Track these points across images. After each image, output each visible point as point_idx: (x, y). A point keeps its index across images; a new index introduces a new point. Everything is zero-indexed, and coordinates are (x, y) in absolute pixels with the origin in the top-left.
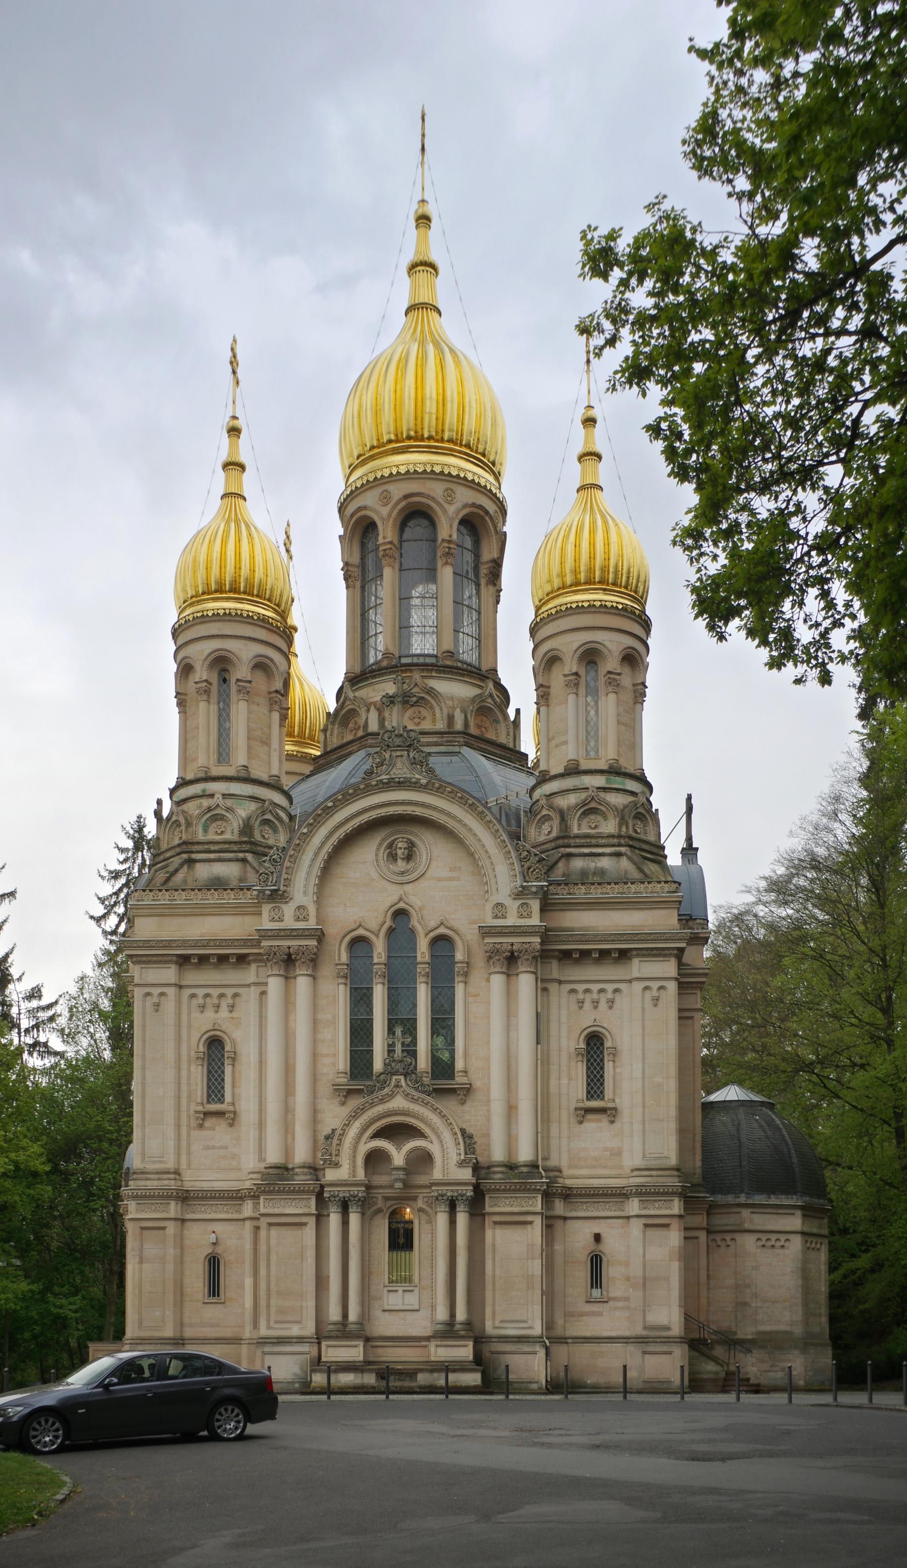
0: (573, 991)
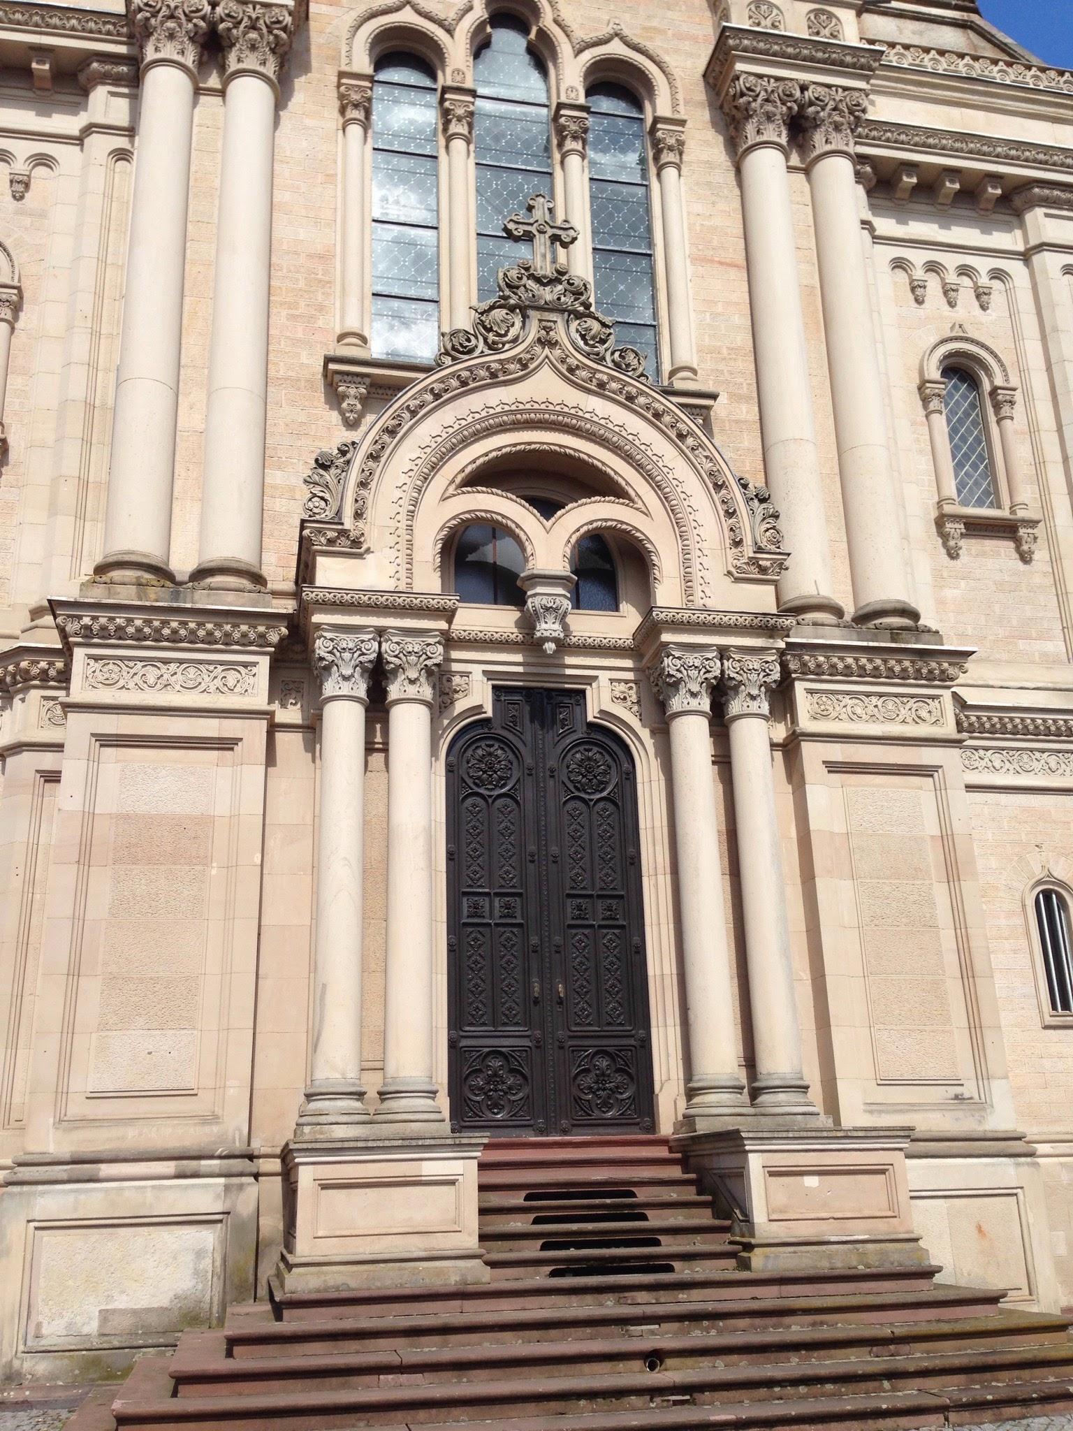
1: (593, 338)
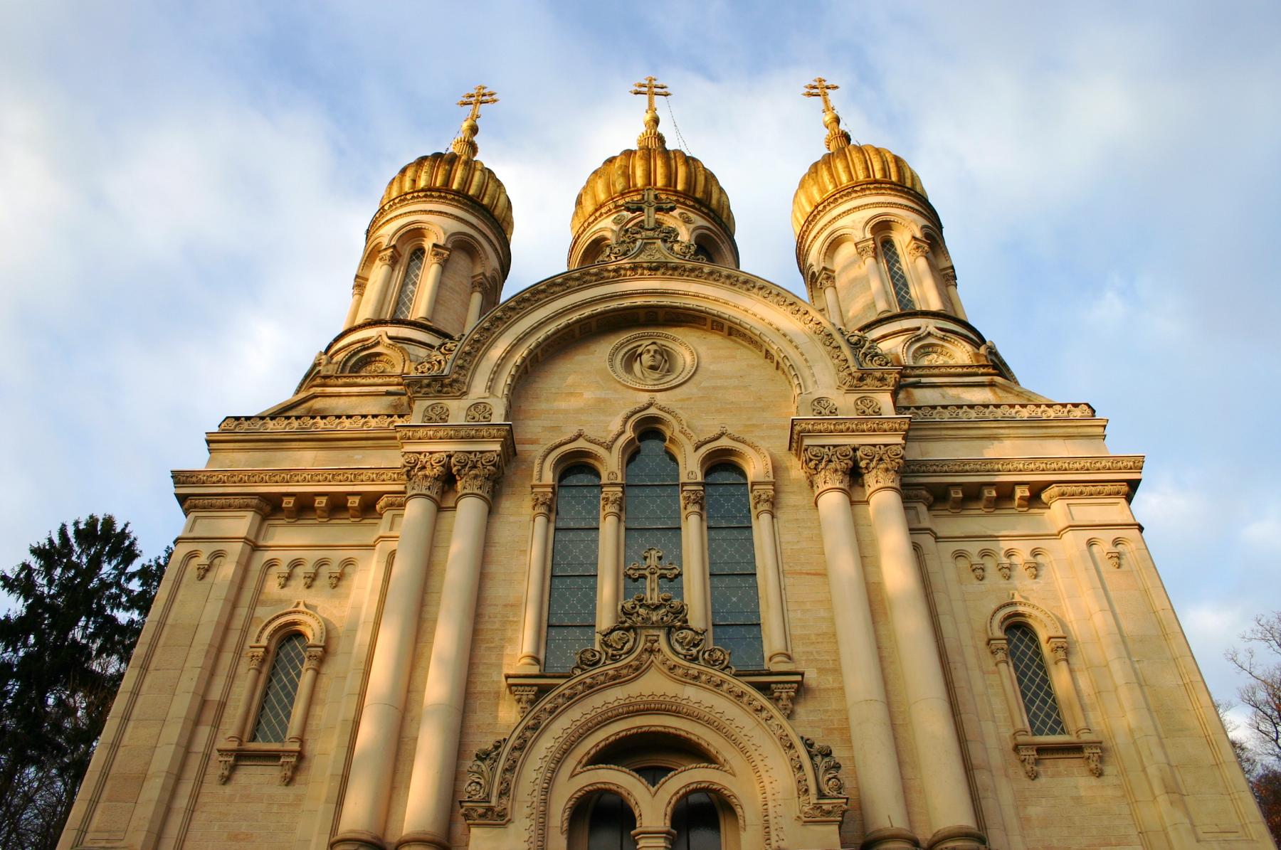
0: (959, 555)
1: (688, 643)
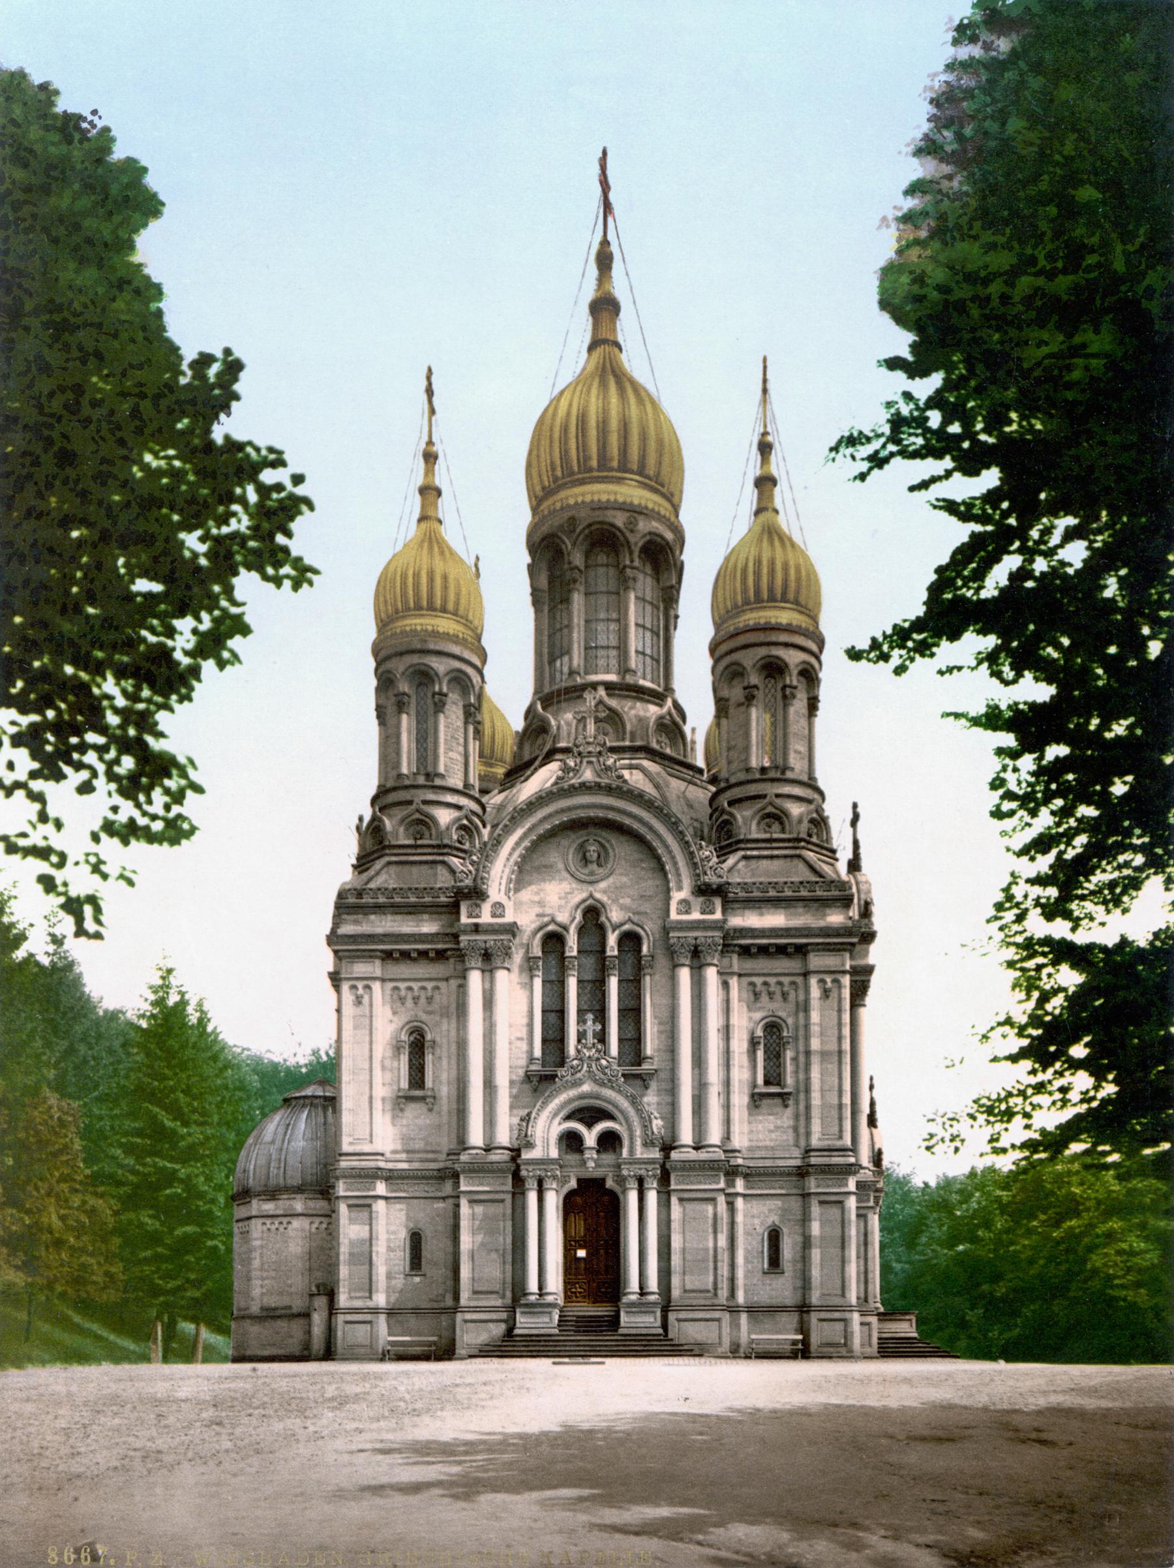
0: (752, 984)
